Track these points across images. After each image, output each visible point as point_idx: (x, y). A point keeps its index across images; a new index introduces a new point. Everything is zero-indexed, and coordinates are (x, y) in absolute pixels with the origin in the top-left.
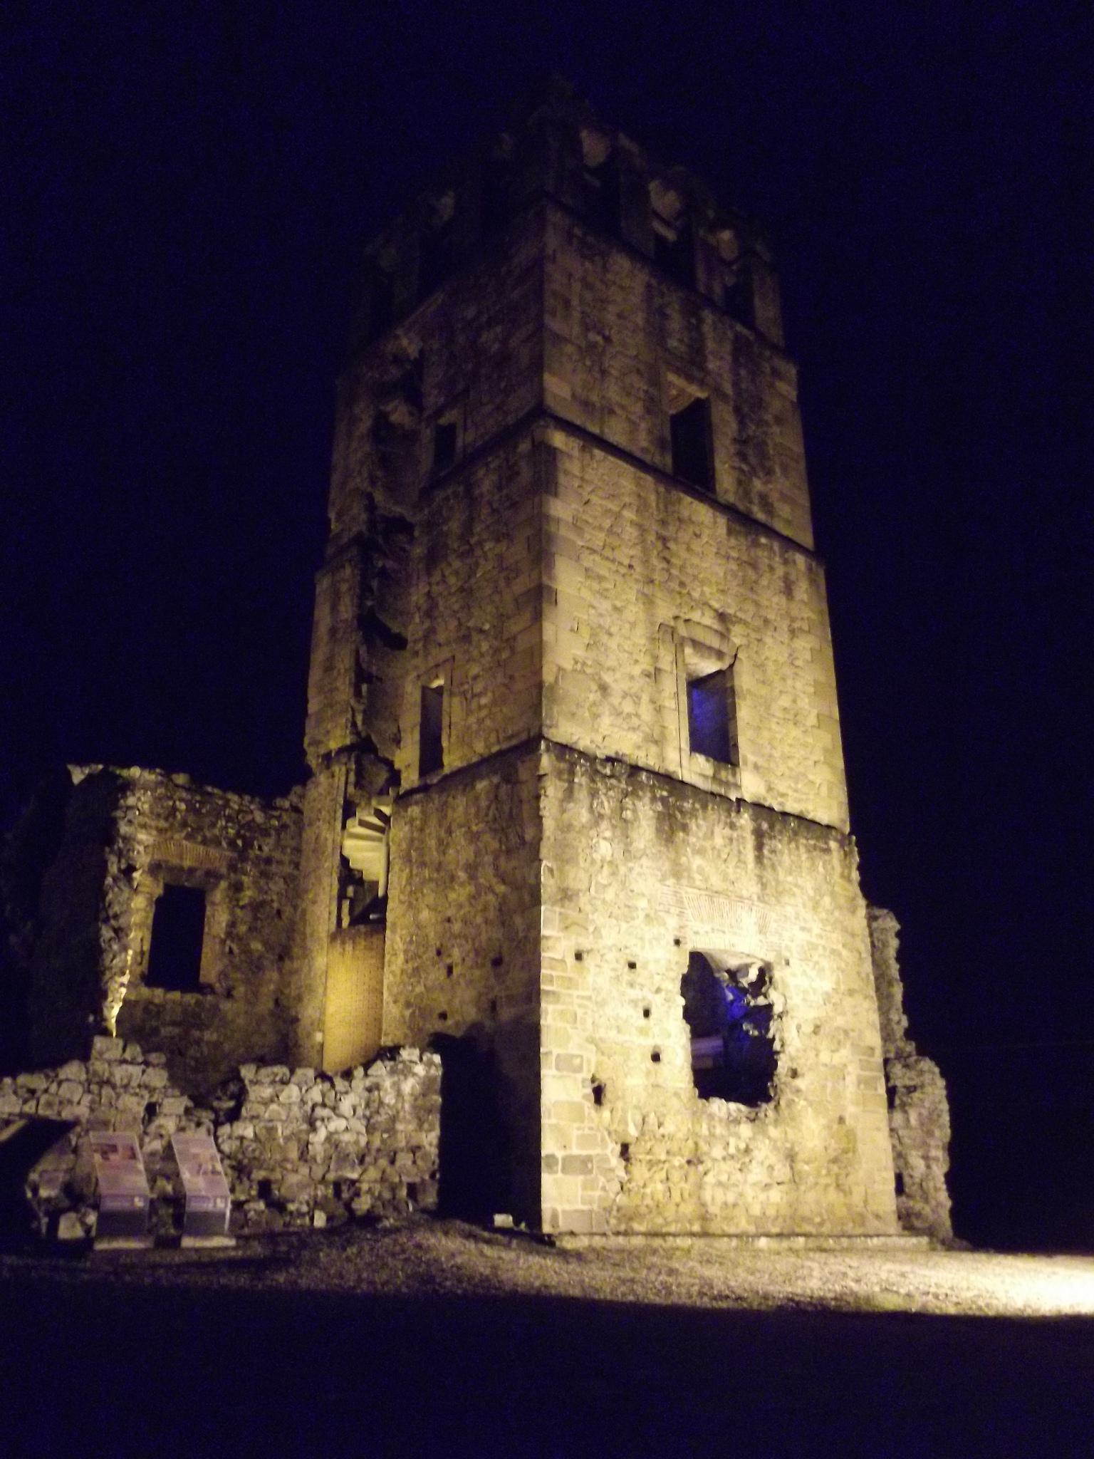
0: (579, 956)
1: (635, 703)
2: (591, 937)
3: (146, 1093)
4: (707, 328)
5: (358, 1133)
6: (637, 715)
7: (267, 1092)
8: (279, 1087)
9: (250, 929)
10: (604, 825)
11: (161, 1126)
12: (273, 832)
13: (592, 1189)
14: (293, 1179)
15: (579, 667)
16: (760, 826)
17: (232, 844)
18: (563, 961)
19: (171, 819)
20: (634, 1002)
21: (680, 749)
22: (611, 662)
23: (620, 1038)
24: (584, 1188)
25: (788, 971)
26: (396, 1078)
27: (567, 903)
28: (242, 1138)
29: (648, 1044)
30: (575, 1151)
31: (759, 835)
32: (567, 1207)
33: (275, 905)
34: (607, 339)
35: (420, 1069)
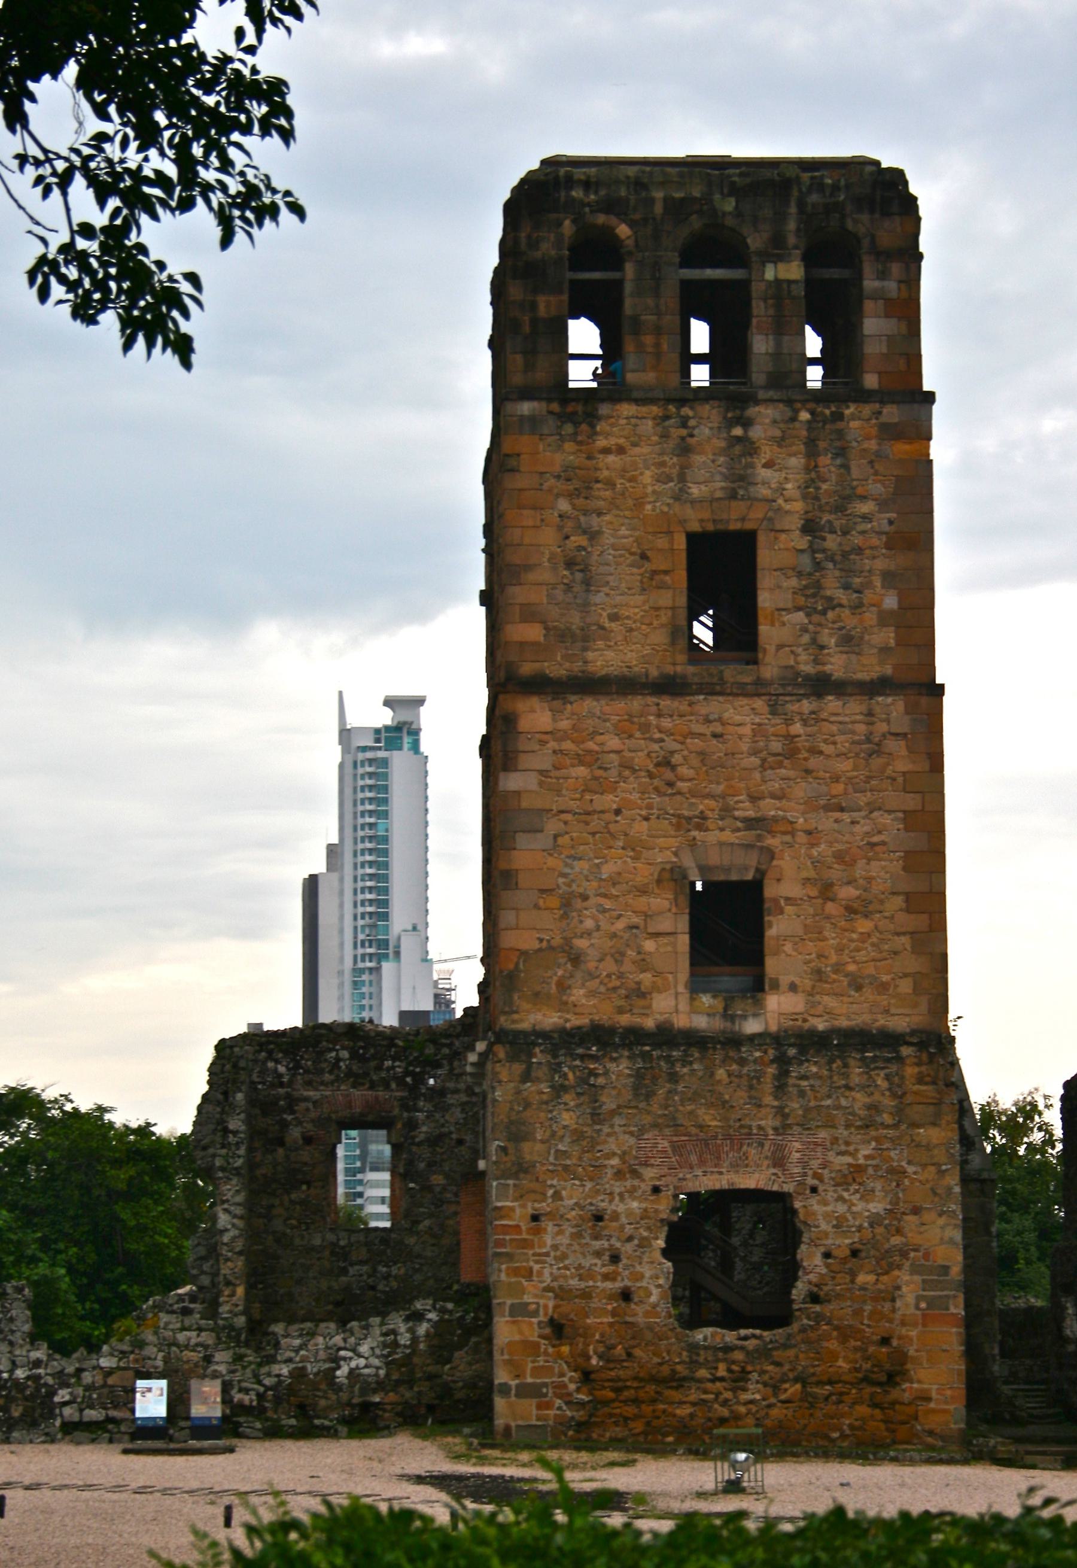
0: (535, 1218)
1: (616, 961)
2: (550, 1200)
3: (200, 1349)
5: (378, 1368)
6: (621, 976)
7: (297, 1342)
9: (430, 1165)
10: (568, 1098)
11: (216, 1371)
12: (445, 1062)
15: (544, 944)
16: (784, 1054)
17: (401, 1082)
18: (518, 1226)
19: (336, 1072)
20: (598, 1254)
22: (589, 924)
23: (583, 1285)
24: (539, 1407)
26: (411, 1324)
27: (522, 1175)
28: (278, 1376)
29: (618, 1285)
30: (529, 1380)
31: (783, 1062)
32: (521, 1423)
33: (454, 1136)
34: (593, 536)
35: (432, 1316)
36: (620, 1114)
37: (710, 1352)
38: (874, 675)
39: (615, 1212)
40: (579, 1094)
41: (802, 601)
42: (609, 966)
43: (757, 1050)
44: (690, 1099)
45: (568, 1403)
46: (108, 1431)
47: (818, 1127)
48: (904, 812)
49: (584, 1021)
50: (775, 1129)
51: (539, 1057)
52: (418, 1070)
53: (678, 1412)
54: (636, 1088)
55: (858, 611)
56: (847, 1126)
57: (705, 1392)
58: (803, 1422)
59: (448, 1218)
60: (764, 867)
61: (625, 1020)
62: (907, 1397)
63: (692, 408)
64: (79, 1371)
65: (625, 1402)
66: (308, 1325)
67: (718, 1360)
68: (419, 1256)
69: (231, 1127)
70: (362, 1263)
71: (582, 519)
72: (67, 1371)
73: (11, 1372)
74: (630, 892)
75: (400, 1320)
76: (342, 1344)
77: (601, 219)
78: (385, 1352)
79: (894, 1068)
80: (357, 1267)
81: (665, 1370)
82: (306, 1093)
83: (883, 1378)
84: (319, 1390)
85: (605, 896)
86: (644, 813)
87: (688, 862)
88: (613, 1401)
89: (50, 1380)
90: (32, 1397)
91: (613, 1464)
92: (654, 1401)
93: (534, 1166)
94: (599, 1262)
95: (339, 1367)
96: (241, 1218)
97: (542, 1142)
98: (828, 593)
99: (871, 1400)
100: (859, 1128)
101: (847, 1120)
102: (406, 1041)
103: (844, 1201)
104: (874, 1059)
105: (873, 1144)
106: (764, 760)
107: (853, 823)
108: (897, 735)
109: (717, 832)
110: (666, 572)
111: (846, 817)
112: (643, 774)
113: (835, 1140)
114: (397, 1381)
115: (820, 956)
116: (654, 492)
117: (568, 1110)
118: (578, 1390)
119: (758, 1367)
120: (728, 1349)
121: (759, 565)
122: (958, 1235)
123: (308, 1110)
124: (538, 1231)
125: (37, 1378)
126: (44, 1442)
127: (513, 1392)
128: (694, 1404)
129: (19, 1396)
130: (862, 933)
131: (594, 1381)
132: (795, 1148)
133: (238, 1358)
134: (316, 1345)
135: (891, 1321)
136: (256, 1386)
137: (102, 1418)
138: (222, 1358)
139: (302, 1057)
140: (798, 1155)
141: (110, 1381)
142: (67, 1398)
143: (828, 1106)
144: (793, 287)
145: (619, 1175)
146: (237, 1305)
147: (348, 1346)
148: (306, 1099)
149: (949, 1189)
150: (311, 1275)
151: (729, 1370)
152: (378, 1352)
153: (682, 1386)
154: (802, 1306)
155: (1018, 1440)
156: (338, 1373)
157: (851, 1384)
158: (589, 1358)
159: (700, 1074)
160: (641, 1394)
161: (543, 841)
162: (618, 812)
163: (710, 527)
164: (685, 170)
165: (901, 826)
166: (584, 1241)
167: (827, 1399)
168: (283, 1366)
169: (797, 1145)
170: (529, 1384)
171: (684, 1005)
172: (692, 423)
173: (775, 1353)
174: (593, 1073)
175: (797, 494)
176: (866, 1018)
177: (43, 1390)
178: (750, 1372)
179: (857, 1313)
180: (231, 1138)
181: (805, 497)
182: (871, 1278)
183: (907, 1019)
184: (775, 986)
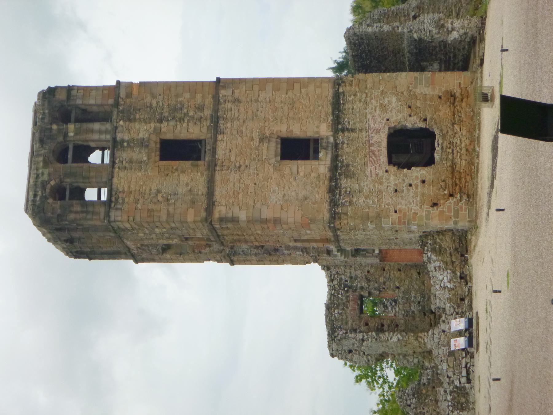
0: (396, 212)
1: (307, 185)
3: (440, 334)
4: (126, 137)
5: (448, 273)
6: (312, 183)
7: (438, 300)
8: (437, 297)
9: (376, 283)
11: (448, 329)
14: (460, 292)
15: (299, 208)
16: (341, 129)
17: (347, 292)
19: (342, 314)
20: (409, 190)
21: (319, 165)
22: (293, 194)
23: (419, 196)
24: (462, 211)
25: (392, 120)
26: (432, 262)
27: (380, 216)
28: (450, 307)
29: (420, 185)
30: (452, 214)
31: (343, 130)
33: (366, 274)
34: (159, 191)
35: (429, 254)
36: (360, 183)
38: (212, 100)
39: (394, 185)
40: (353, 197)
41: (185, 125)
44: (355, 160)
45: (461, 201)
46: (470, 366)
49: (327, 196)
50: (366, 132)
51: (339, 210)
52: (343, 286)
53: (464, 164)
54: (351, 178)
55: (189, 105)
56: (366, 109)
57: (457, 156)
58: (467, 124)
59: (395, 276)
60: (276, 136)
61: (327, 182)
62: (459, 91)
63: (116, 159)
64: (448, 377)
66: (432, 297)
67: (446, 151)
68: (408, 287)
69: (361, 337)
70: (410, 306)
71: (152, 196)
72: (448, 381)
73: (448, 401)
74: (283, 180)
75: (431, 265)
76: (439, 285)
77: (48, 191)
78: (442, 270)
80: (412, 308)
81: (449, 169)
82: (350, 324)
83: (453, 98)
84: (455, 294)
85: (284, 188)
86: (255, 175)
87: (273, 161)
88: (460, 186)
89: (452, 387)
90: (458, 393)
91: (482, 77)
92: (460, 173)
93: (377, 212)
94: (411, 190)
95: (447, 286)
96: (394, 334)
97: (369, 208)
98: (183, 115)
100: (366, 105)
101: (364, 109)
102: (333, 290)
103: (392, 110)
104: (343, 100)
105: (372, 101)
106: (240, 136)
108: (233, 93)
109: (263, 151)
110: (172, 168)
111: (260, 109)
112: (242, 176)
113: (371, 113)
114: (452, 267)
115: (308, 118)
116: (144, 172)
117: (358, 200)
118: (456, 198)
120: (442, 148)
122: (404, 74)
123: (356, 324)
124: (400, 210)
125: (451, 392)
126: (474, 389)
127: (456, 219)
128: (461, 159)
129: (457, 398)
131: (453, 192)
132: (373, 125)
133: (444, 322)
134: (439, 294)
135: (433, 95)
136: (454, 315)
137: (465, 369)
138: (443, 326)
139: (337, 326)
141: (451, 366)
142: (458, 381)
143: (359, 115)
144: (77, 127)
145: (381, 183)
146: (425, 335)
147: (440, 283)
148: (352, 324)
149: (388, 76)
150: (414, 323)
151: (450, 148)
152: (442, 273)
155: (475, 57)
156: (449, 287)
158: (445, 194)
159: (346, 156)
160: (457, 177)
161: (264, 209)
162: (255, 184)
163: (158, 153)
164: (33, 163)
165: (264, 92)
166: (404, 195)
168: (446, 305)
169: (372, 125)
171: (323, 163)
172: (121, 159)
173: (444, 133)
174: (345, 192)
175: (149, 125)
176: (329, 103)
177: (455, 390)
179: (430, 106)
180: (365, 337)
181: (150, 123)
182: (418, 101)
183: (330, 90)
184: (317, 132)
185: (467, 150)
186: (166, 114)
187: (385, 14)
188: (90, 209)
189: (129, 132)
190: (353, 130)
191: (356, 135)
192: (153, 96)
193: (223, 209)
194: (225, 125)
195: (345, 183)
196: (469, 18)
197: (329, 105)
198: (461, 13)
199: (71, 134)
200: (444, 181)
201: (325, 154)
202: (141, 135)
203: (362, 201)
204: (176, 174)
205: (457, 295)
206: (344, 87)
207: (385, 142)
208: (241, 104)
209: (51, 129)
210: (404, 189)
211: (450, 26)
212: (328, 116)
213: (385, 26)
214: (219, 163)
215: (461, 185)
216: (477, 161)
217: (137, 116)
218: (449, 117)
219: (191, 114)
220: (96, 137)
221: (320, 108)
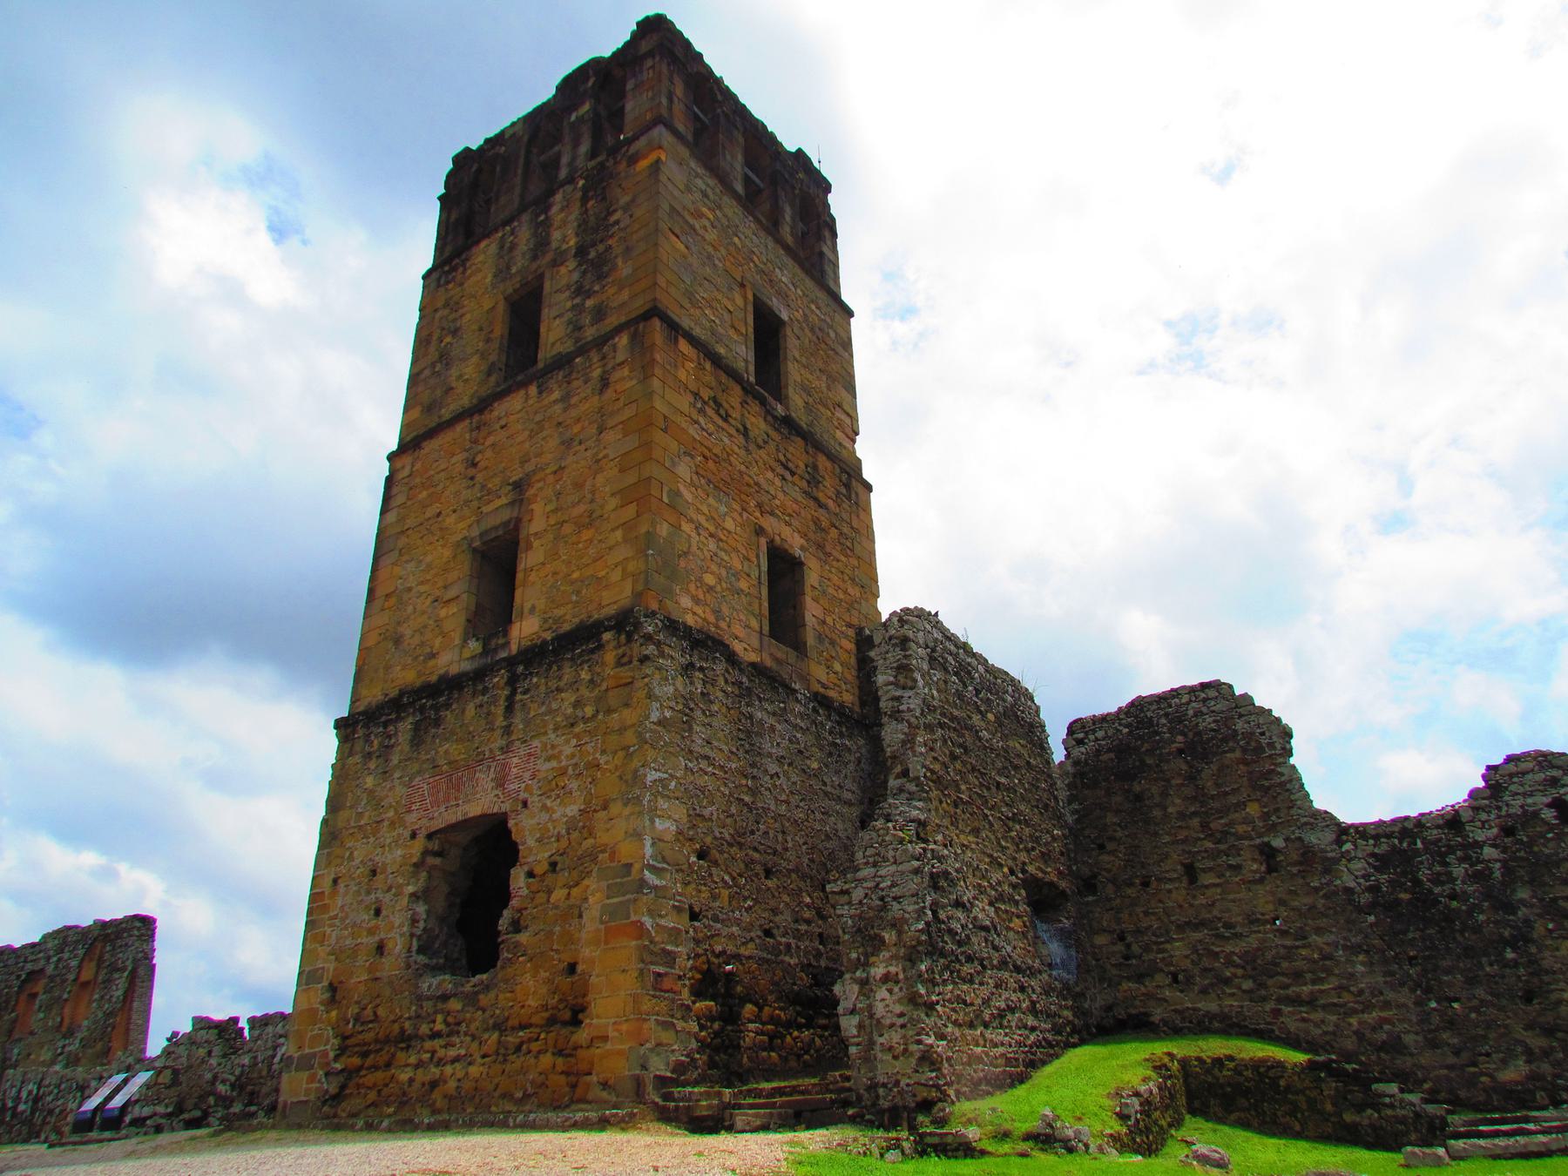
0: (335, 881)
1: (421, 633)
4: (555, 209)
13: (312, 1082)
24: (307, 1083)
28: (243, 1066)
29: (377, 938)
31: (512, 682)
32: (295, 1100)
37: (430, 1003)
39: (383, 862)
40: (378, 757)
42: (417, 640)
43: (496, 676)
45: (327, 1074)
47: (532, 736)
48: (622, 423)
51: (360, 732)
54: (411, 741)
58: (496, 1081)
65: (368, 1069)
67: (436, 1012)
77: (491, 153)
79: (595, 656)
81: (396, 1027)
83: (567, 1015)
84: (261, 1077)
85: (422, 583)
92: (388, 1065)
97: (351, 807)
98: (587, 287)
99: (555, 1047)
104: (581, 655)
105: (574, 742)
107: (586, 450)
108: (623, 363)
111: (583, 447)
119: (468, 1015)
120: (445, 998)
121: (544, 293)
124: (334, 893)
130: (586, 541)
136: (230, 1077)
140: (515, 770)
145: (392, 823)
153: (408, 1047)
154: (505, 937)
157: (541, 1027)
158: (348, 1023)
163: (518, 286)
165: (620, 436)
167: (518, 1048)
169: (515, 760)
170: (307, 1054)
173: (481, 997)
175: (573, 235)
178: (459, 1024)
181: (577, 235)
185: (434, 1084)
186: (593, 254)
187: (1259, 749)
188: (450, 238)
189: (562, 210)
190: (509, 709)
191: (500, 721)
192: (626, 208)
193: (406, 472)
194: (555, 386)
195: (405, 727)
196: (913, 1047)
197: (577, 620)
198: (1317, 1016)
199: (573, 118)
200: (375, 1014)
201: (474, 654)
202: (556, 235)
203: (367, 786)
204: (481, 344)
205: (260, 1083)
206: (615, 643)
207: (474, 810)
208: (597, 397)
209: (588, 80)
210: (373, 896)
211: (878, 971)
212: (555, 627)
213: (904, 727)
214: (486, 416)
215: (363, 1073)
216: (360, 1123)
217: (591, 203)
218: (515, 1008)
219: (589, 303)
220: (565, 160)
221: (574, 598)
